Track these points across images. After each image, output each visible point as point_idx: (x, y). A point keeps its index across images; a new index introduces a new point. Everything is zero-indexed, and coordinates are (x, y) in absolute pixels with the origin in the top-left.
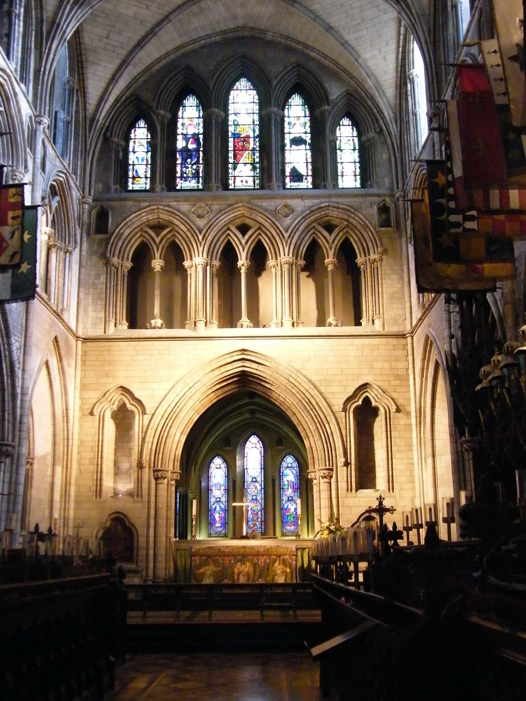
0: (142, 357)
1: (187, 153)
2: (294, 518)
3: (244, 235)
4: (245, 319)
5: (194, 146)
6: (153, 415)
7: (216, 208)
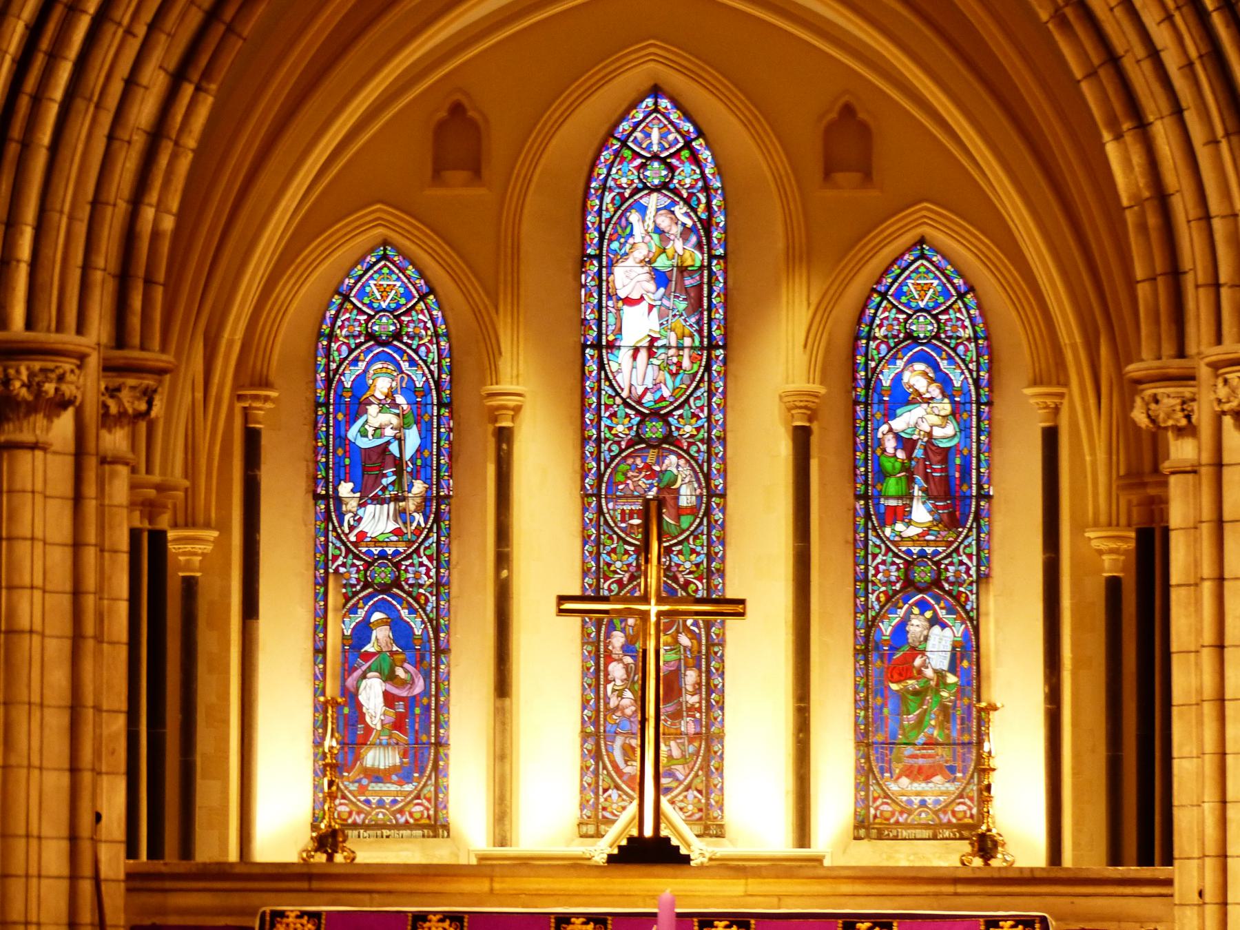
2: (946, 712)
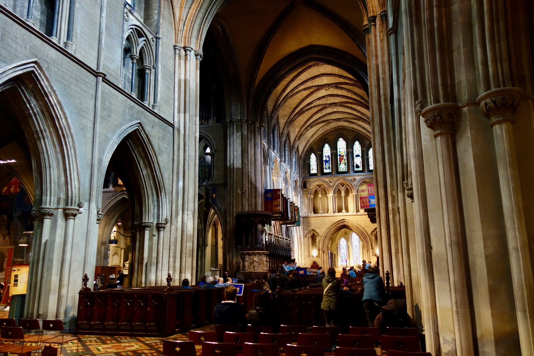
0: (318, 222)
1: (326, 161)
3: (343, 187)
4: (344, 211)
5: (328, 159)
6: (321, 237)
7: (335, 180)
